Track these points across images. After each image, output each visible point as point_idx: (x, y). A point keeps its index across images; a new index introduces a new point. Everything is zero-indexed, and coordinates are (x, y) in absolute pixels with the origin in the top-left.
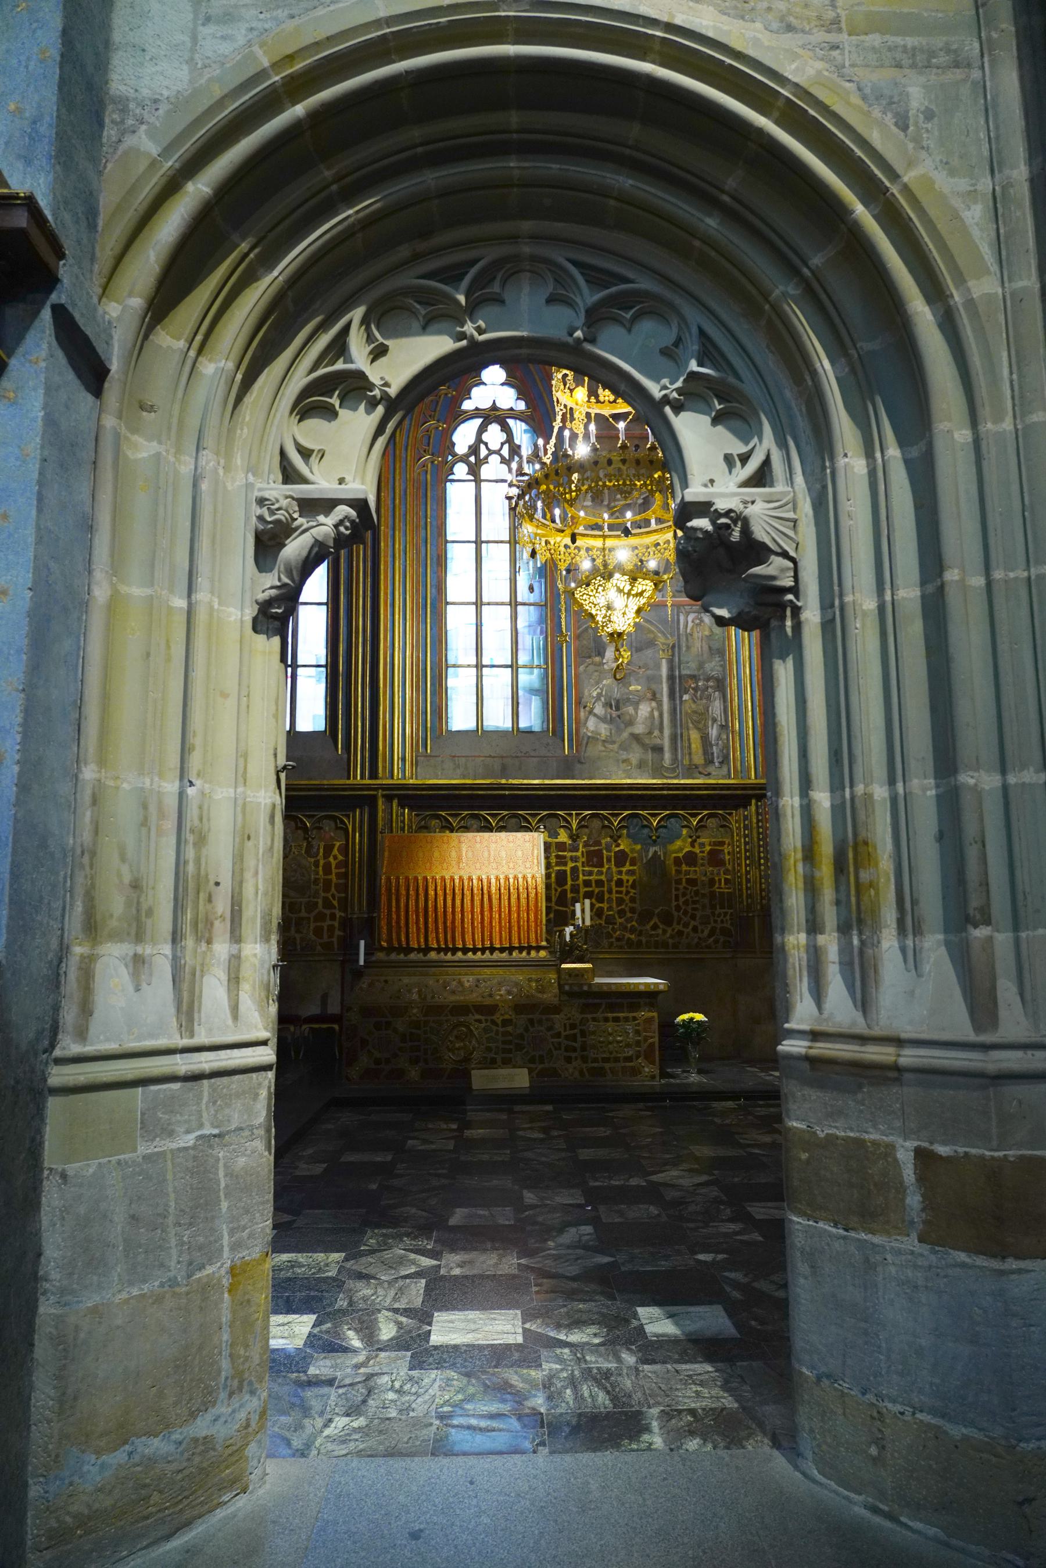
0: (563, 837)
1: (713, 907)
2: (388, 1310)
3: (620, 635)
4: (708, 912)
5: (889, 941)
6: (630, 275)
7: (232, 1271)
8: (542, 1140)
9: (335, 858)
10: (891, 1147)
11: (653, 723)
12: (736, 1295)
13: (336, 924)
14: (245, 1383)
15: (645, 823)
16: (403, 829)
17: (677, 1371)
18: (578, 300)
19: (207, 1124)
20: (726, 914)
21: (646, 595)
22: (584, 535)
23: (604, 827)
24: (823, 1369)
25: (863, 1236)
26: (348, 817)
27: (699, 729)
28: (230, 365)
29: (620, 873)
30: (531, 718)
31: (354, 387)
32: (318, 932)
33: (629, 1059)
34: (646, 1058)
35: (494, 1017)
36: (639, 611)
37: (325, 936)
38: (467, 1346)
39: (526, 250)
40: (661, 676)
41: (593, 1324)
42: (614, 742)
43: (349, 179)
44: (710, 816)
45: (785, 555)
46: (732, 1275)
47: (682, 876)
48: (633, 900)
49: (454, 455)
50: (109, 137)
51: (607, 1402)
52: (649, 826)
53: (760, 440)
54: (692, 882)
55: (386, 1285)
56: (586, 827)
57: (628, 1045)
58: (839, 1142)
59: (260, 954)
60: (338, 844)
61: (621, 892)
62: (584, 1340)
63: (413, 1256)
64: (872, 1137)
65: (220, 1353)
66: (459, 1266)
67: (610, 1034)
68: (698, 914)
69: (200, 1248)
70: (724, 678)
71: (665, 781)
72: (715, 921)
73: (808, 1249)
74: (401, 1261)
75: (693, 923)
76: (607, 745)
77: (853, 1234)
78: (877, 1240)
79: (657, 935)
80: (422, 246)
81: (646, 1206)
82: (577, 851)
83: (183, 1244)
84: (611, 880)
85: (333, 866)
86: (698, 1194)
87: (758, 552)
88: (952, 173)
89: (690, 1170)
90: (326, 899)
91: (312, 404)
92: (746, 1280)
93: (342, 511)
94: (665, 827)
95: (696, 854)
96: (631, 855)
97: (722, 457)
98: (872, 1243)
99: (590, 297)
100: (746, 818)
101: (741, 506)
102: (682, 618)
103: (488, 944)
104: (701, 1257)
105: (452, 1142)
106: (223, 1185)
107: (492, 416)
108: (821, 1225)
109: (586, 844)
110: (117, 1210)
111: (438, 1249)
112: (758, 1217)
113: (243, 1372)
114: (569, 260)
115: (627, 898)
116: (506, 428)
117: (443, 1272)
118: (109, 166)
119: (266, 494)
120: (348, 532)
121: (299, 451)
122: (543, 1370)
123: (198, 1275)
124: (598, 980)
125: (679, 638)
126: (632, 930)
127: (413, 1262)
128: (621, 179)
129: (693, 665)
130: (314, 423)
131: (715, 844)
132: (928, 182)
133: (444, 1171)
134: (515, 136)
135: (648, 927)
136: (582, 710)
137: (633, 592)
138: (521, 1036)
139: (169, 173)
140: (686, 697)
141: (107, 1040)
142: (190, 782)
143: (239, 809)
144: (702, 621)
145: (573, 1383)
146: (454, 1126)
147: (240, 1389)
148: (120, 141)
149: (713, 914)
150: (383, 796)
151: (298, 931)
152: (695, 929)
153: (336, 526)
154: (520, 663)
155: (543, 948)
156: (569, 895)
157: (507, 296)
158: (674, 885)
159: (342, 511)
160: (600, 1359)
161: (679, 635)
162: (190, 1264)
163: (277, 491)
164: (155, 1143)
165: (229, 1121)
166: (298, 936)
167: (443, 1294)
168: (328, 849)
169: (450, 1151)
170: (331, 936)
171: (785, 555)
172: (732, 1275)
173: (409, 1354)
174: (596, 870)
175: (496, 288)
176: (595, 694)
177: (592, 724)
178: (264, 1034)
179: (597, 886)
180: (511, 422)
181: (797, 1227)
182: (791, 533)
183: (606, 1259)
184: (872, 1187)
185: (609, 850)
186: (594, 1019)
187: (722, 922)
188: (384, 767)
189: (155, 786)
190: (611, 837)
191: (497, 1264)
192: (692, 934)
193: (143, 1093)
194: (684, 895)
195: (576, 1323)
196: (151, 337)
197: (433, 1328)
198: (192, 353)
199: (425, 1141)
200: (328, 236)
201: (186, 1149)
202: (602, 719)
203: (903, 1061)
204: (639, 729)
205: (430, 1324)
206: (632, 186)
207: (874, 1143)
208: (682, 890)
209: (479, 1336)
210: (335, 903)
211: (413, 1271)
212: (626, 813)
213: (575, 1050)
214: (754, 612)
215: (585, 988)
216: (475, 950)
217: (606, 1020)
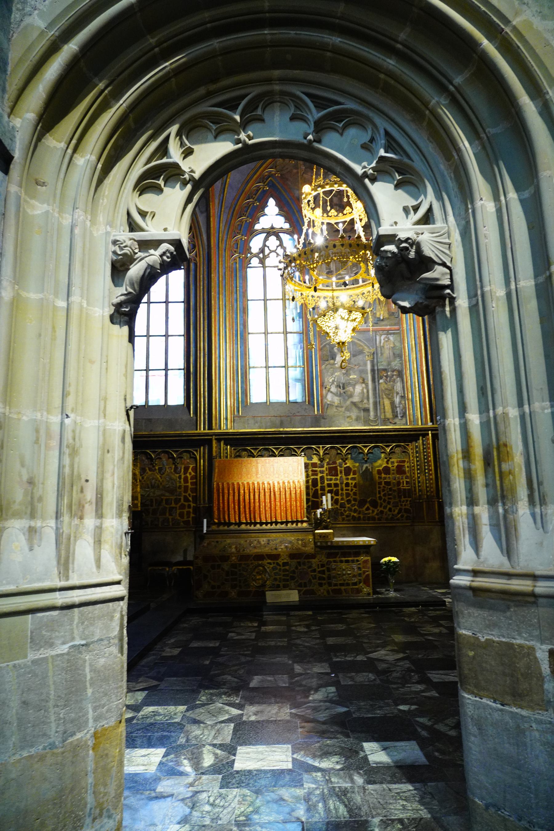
0: (315, 460)
1: (400, 497)
2: (210, 745)
3: (343, 343)
4: (397, 500)
5: (523, 510)
6: (341, 100)
7: (95, 735)
8: (305, 633)
9: (190, 474)
10: (532, 649)
11: (363, 395)
12: (424, 733)
13: (191, 510)
14: (105, 811)
16: (227, 457)
17: (390, 790)
18: (310, 117)
19: (77, 637)
20: (407, 501)
21: (357, 320)
22: (322, 290)
23: (338, 454)
24: (490, 801)
25: (514, 709)
26: (197, 451)
27: (389, 399)
28: (94, 158)
29: (347, 479)
30: (296, 395)
31: (172, 173)
32: (182, 515)
33: (355, 584)
34: (365, 583)
37: (185, 517)
38: (257, 770)
39: (277, 88)
41: (336, 755)
42: (342, 407)
43: (165, 45)
44: (396, 446)
45: (444, 265)
46: (421, 720)
47: (382, 480)
48: (355, 494)
49: (251, 253)
50: (15, 18)
51: (345, 813)
52: (363, 453)
53: (426, 197)
54: (388, 483)
55: (209, 727)
56: (328, 454)
57: (354, 576)
58: (495, 644)
59: (116, 526)
60: (191, 466)
61: (348, 490)
62: (331, 766)
63: (227, 708)
64: (518, 642)
65: (86, 792)
66: (255, 714)
67: (344, 570)
68: (392, 501)
69: (72, 721)
70: (402, 371)
71: (371, 427)
72: (401, 505)
73: (476, 717)
74: (220, 711)
75: (389, 506)
77: (507, 708)
78: (524, 713)
79: (369, 513)
80: (212, 87)
81: (367, 674)
82: (323, 467)
83: (60, 719)
86: (398, 666)
87: (426, 263)
88: (544, 17)
90: (185, 496)
91: (147, 184)
92: (429, 723)
93: (165, 247)
94: (372, 453)
96: (353, 469)
97: (402, 209)
98: (521, 715)
99: (315, 114)
101: (415, 236)
102: (378, 338)
103: (274, 520)
104: (402, 707)
105: (254, 634)
106: (88, 677)
107: (272, 232)
108: (484, 700)
109: (328, 464)
110: (13, 698)
111: (243, 703)
112: (435, 680)
113: (103, 803)
115: (351, 493)
116: (279, 238)
117: (244, 718)
118: (15, 35)
119: (118, 238)
120: (169, 260)
121: (139, 213)
122: (304, 789)
123: (70, 740)
124: (336, 539)
125: (376, 349)
126: (355, 511)
127: (227, 712)
128: (334, 38)
129: (385, 363)
130: (149, 197)
131: (400, 462)
132: (529, 24)
134: (267, 15)
135: (364, 509)
138: (294, 572)
139: (52, 38)
140: (381, 381)
141: (8, 583)
142: (67, 415)
143: (101, 433)
144: (389, 339)
145: (324, 799)
146: (256, 625)
147: (101, 815)
148: (22, 20)
149: (400, 501)
150: (216, 439)
151: (170, 515)
152: (390, 510)
153: (161, 256)
154: (290, 365)
156: (320, 492)
157: (266, 117)
158: (377, 486)
159: (165, 247)
160: (340, 781)
161: (376, 347)
162: (65, 732)
163: (125, 236)
164: (40, 652)
165: (93, 635)
167: (245, 733)
168: (186, 469)
169: (252, 640)
170: (188, 517)
171: (444, 265)
172: (421, 720)
173: (220, 776)
174: (334, 478)
175: (259, 112)
176: (331, 381)
177: (329, 397)
178: (117, 577)
180: (281, 235)
181: (468, 701)
182: (447, 251)
183: (344, 709)
184: (519, 676)
185: (341, 467)
186: (335, 562)
187: (405, 505)
188: (216, 424)
189: (44, 419)
191: (277, 713)
192: (389, 513)
193: (32, 618)
194: (384, 490)
195: (325, 754)
196: (43, 140)
197: (237, 758)
198: (70, 151)
199: (239, 634)
200: (153, 79)
201: (62, 655)
202: (335, 394)
203: (538, 590)
204: (356, 399)
205: (234, 755)
206: (340, 42)
207: (521, 646)
209: (265, 763)
210: (190, 499)
211: (226, 718)
213: (324, 579)
215: (329, 544)
216: (267, 524)
217: (341, 562)
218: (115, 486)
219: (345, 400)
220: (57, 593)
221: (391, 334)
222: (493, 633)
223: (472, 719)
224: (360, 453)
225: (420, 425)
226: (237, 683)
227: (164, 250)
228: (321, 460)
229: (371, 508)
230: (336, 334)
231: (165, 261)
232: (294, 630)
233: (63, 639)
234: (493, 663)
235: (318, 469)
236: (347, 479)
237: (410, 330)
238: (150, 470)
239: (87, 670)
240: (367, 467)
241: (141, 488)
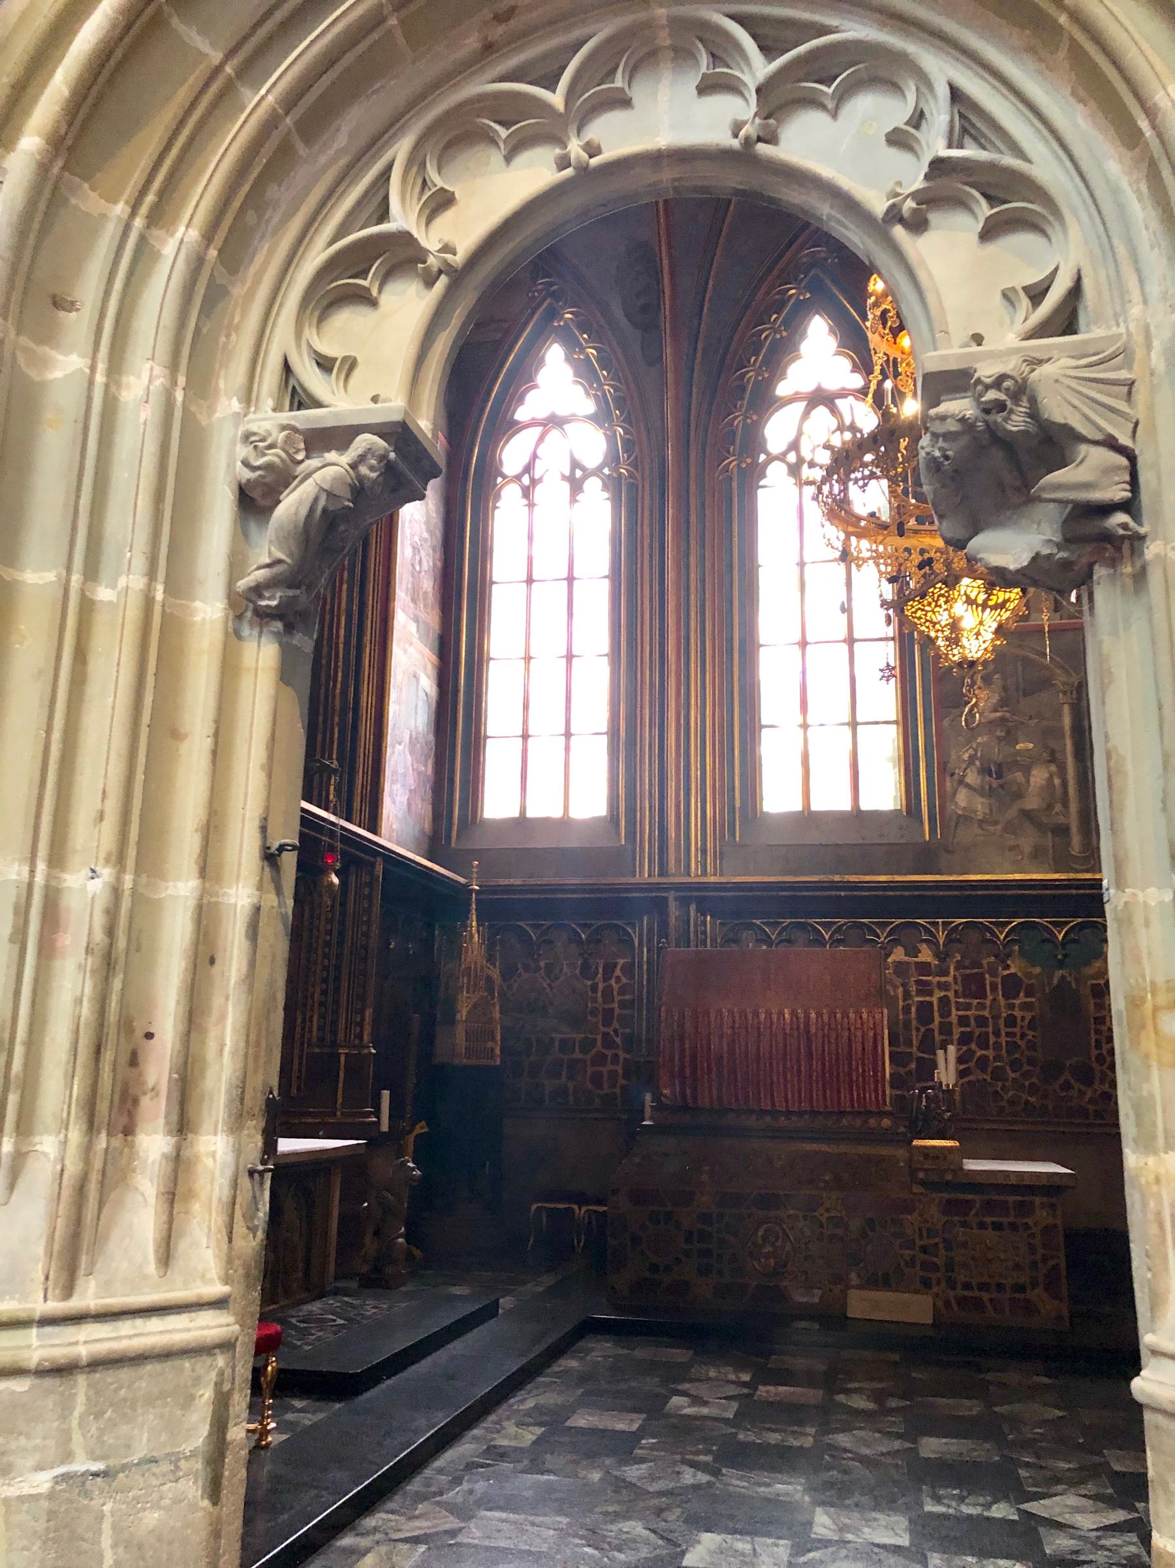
0: (926, 955)
3: (972, 664)
9: (618, 979)
15: (1046, 935)
16: (704, 943)
18: (746, 78)
19: (80, 1453)
21: (1011, 606)
22: (916, 532)
26: (634, 927)
29: (1012, 1007)
32: (597, 1079)
33: (1021, 1288)
36: (1000, 631)
40: (1062, 728)
42: (996, 823)
45: (1111, 443)
48: (1032, 1046)
49: (768, 454)
52: (1052, 939)
57: (1017, 1267)
60: (621, 962)
61: (1013, 1035)
67: (989, 1249)
71: (1072, 876)
76: (986, 827)
80: (498, 32)
82: (946, 974)
84: (1000, 1017)
85: (615, 993)
87: (1054, 444)
89: (1096, 1498)
90: (606, 1035)
94: (1074, 941)
103: (805, 1106)
105: (735, 1405)
107: (821, 398)
114: (732, 17)
116: (834, 411)
119: (254, 427)
120: (374, 475)
121: (318, 364)
126: (1033, 1089)
133: (708, 1458)
136: (948, 779)
137: (990, 603)
142: (93, 871)
146: (746, 1377)
150: (676, 899)
153: (354, 466)
156: (938, 1037)
157: (638, 93)
163: (269, 419)
165: (128, 1446)
166: (571, 1085)
168: (609, 969)
169: (726, 1421)
171: (1111, 443)
175: (619, 82)
176: (966, 757)
178: (218, 1289)
182: (1122, 405)
185: (994, 973)
186: (964, 1224)
188: (678, 861)
190: (996, 957)
198: (138, 223)
199: (697, 1401)
202: (980, 791)
204: (1032, 802)
213: (935, 1267)
214: (1063, 554)
215: (949, 1177)
217: (982, 1226)
218: (227, 1049)
220: (34, 1331)
227: (360, 451)
228: (942, 956)
229: (1077, 1085)
230: (954, 641)
231: (365, 477)
232: (841, 1405)
233: (38, 1456)
236: (1012, 1007)
238: (526, 968)
239: (106, 1541)
240: (1063, 977)
241: (501, 1012)
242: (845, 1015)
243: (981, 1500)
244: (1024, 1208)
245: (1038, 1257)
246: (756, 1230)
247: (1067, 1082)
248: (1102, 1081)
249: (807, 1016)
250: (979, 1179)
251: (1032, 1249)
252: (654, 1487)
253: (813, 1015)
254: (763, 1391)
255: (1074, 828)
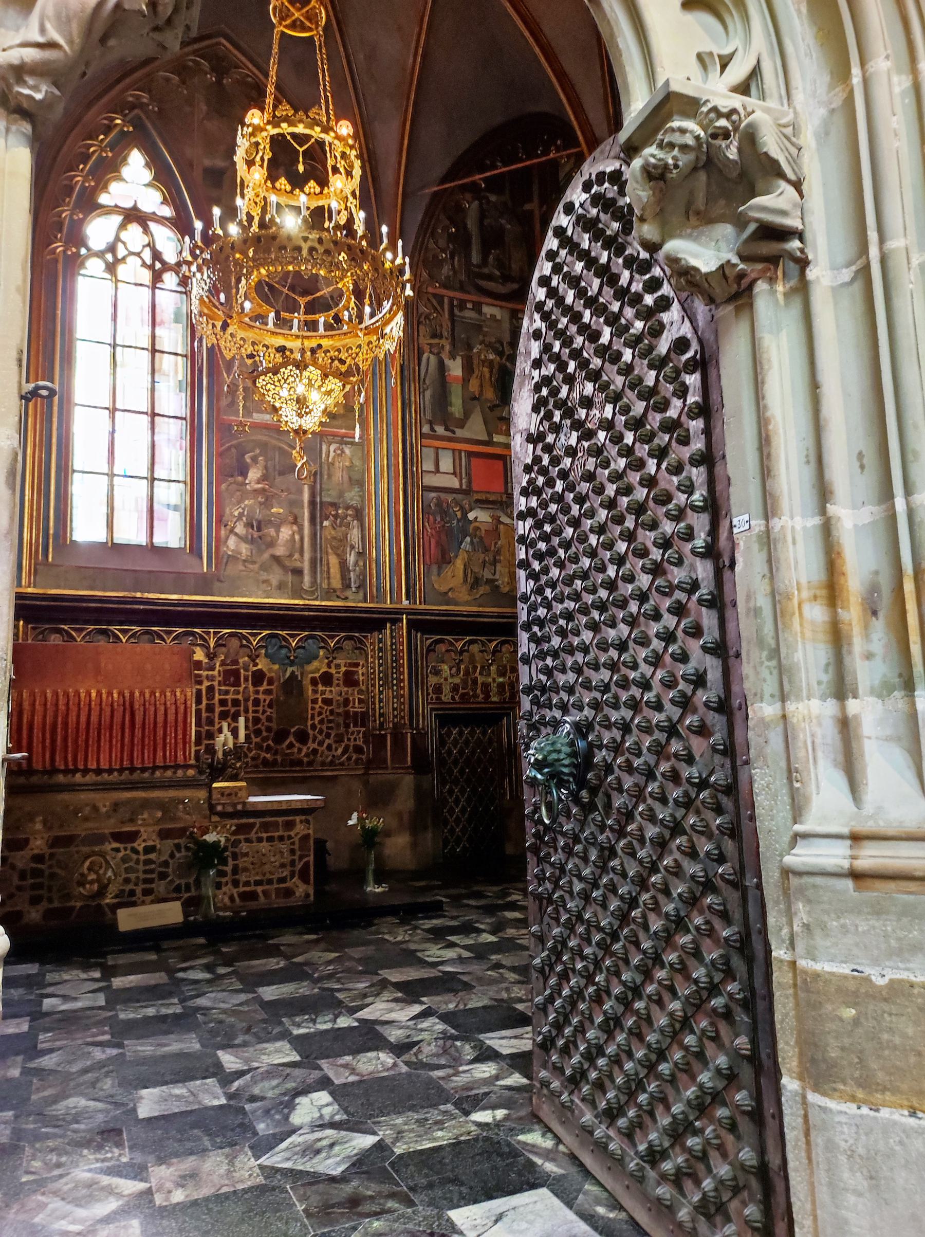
1: (347, 726)
3: (305, 432)
4: (342, 730)
8: (208, 981)
20: (359, 732)
23: (242, 646)
27: (338, 555)
29: (257, 692)
33: (282, 880)
35: (135, 845)
40: (302, 501)
42: (254, 563)
45: (797, 185)
47: (318, 696)
48: (269, 719)
49: (88, 249)
52: (288, 647)
54: (327, 702)
56: (224, 645)
57: (283, 866)
58: (916, 991)
70: (363, 509)
72: (349, 740)
73: (861, 1151)
79: (293, 754)
82: (213, 669)
86: (422, 1030)
89: (396, 1000)
94: (304, 648)
95: (331, 675)
96: (268, 675)
100: (380, 641)
102: (324, 447)
108: (885, 1113)
109: (223, 663)
116: (146, 230)
124: (252, 799)
125: (321, 466)
127: (110, 1191)
129: (333, 493)
131: (351, 665)
138: (166, 864)
140: (326, 523)
144: (343, 452)
152: (329, 748)
155: (191, 766)
158: (310, 705)
161: (321, 463)
176: (236, 513)
177: (232, 542)
179: (233, 706)
180: (152, 226)
181: (837, 1119)
185: (246, 670)
186: (248, 840)
187: (355, 740)
190: (249, 657)
191: (229, 1171)
192: (326, 752)
194: (320, 714)
199: (65, 998)
204: (280, 551)
208: (318, 710)
212: (265, 633)
214: (741, 266)
215: (239, 807)
216: (110, 771)
217: (260, 840)
219: (260, 552)
221: (347, 443)
222: (911, 965)
223: (850, 1157)
224: (281, 647)
225: (388, 605)
226: (107, 1112)
228: (211, 656)
232: (184, 980)
234: (910, 1031)
235: (205, 673)
236: (257, 692)
237: (382, 441)
240: (293, 672)
242: (163, 693)
243: (327, 1018)
244: (290, 825)
245: (296, 857)
246: (83, 862)
247: (291, 743)
248: (314, 741)
249: (132, 694)
250: (260, 808)
251: (293, 852)
252: (74, 1068)
253: (137, 694)
254: (118, 982)
255: (306, 571)
